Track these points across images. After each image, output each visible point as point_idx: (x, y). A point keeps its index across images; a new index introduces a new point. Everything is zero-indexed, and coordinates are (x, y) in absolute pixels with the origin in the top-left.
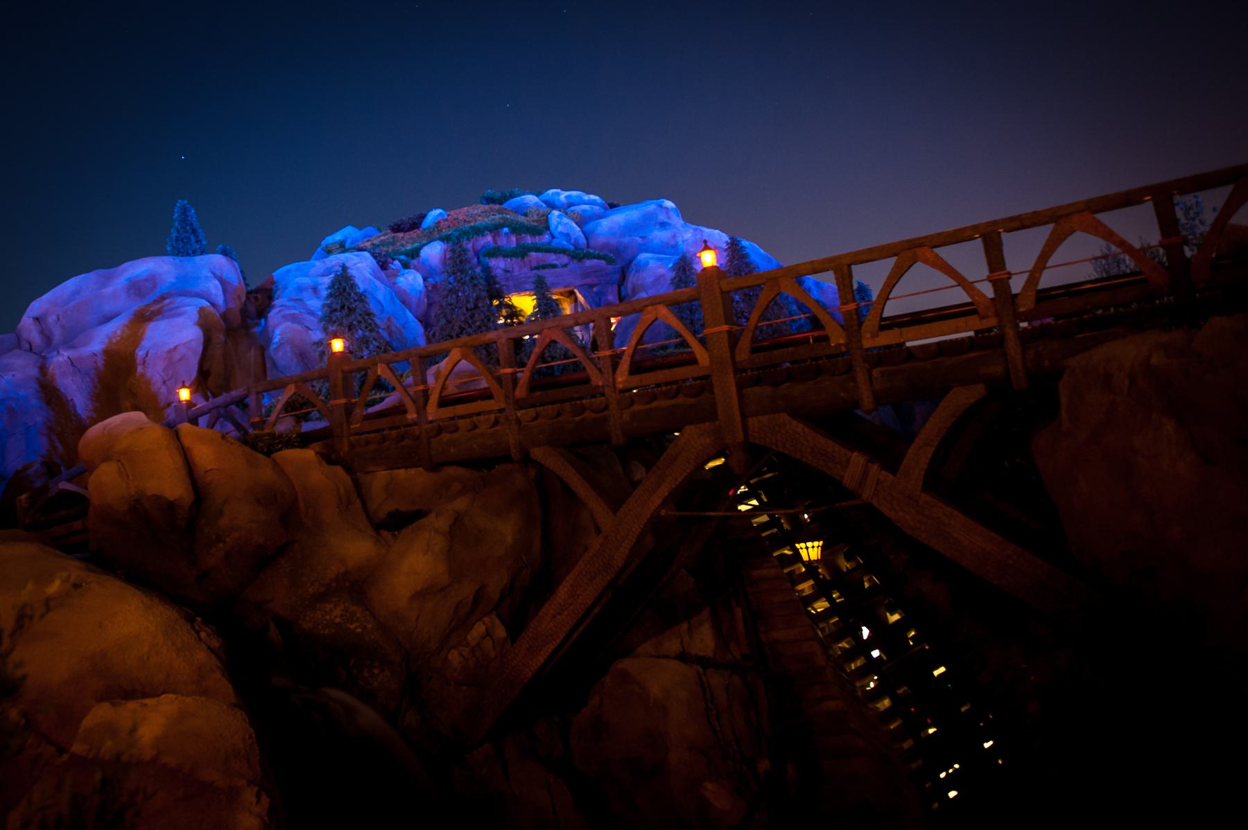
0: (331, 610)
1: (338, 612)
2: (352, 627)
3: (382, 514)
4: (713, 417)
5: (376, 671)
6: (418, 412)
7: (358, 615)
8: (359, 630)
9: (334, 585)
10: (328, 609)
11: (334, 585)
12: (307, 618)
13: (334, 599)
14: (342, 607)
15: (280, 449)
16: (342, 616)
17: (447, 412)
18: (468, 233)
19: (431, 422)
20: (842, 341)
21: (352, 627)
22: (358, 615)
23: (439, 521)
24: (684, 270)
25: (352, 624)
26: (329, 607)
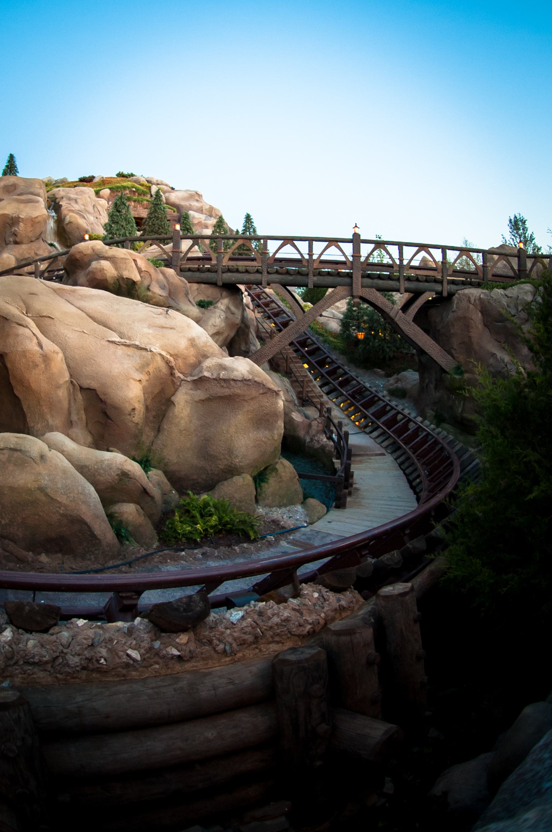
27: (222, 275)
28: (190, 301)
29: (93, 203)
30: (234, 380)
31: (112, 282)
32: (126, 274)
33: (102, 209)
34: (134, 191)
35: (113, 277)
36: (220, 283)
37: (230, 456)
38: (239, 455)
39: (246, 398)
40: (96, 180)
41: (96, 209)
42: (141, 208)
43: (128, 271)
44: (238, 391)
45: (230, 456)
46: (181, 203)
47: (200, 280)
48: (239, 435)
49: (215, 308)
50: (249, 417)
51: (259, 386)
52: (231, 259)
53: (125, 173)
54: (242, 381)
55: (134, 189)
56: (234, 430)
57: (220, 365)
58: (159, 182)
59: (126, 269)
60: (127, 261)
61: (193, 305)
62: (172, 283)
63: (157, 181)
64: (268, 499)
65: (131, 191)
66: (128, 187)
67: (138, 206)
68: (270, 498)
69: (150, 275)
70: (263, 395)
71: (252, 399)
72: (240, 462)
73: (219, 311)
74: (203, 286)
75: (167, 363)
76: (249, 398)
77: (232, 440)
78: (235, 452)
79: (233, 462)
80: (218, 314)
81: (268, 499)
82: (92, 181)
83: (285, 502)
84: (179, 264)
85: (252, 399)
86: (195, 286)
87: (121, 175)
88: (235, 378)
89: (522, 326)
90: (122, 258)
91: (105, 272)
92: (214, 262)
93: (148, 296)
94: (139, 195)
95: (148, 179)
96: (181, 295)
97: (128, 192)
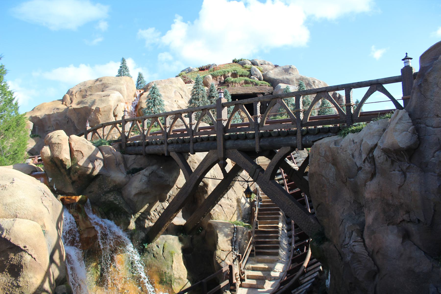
0: (110, 196)
1: (113, 197)
2: (116, 202)
3: (131, 168)
7: (118, 199)
8: (118, 203)
9: (112, 189)
10: (110, 196)
11: (112, 189)
12: (103, 198)
13: (112, 193)
14: (114, 196)
16: (113, 198)
21: (116, 202)
22: (118, 199)
25: (116, 201)
26: (110, 195)
28: (120, 170)
35: (48, 157)
49: (139, 174)
53: (237, 59)
74: (139, 156)
86: (133, 157)
89: (409, 165)
95: (253, 62)
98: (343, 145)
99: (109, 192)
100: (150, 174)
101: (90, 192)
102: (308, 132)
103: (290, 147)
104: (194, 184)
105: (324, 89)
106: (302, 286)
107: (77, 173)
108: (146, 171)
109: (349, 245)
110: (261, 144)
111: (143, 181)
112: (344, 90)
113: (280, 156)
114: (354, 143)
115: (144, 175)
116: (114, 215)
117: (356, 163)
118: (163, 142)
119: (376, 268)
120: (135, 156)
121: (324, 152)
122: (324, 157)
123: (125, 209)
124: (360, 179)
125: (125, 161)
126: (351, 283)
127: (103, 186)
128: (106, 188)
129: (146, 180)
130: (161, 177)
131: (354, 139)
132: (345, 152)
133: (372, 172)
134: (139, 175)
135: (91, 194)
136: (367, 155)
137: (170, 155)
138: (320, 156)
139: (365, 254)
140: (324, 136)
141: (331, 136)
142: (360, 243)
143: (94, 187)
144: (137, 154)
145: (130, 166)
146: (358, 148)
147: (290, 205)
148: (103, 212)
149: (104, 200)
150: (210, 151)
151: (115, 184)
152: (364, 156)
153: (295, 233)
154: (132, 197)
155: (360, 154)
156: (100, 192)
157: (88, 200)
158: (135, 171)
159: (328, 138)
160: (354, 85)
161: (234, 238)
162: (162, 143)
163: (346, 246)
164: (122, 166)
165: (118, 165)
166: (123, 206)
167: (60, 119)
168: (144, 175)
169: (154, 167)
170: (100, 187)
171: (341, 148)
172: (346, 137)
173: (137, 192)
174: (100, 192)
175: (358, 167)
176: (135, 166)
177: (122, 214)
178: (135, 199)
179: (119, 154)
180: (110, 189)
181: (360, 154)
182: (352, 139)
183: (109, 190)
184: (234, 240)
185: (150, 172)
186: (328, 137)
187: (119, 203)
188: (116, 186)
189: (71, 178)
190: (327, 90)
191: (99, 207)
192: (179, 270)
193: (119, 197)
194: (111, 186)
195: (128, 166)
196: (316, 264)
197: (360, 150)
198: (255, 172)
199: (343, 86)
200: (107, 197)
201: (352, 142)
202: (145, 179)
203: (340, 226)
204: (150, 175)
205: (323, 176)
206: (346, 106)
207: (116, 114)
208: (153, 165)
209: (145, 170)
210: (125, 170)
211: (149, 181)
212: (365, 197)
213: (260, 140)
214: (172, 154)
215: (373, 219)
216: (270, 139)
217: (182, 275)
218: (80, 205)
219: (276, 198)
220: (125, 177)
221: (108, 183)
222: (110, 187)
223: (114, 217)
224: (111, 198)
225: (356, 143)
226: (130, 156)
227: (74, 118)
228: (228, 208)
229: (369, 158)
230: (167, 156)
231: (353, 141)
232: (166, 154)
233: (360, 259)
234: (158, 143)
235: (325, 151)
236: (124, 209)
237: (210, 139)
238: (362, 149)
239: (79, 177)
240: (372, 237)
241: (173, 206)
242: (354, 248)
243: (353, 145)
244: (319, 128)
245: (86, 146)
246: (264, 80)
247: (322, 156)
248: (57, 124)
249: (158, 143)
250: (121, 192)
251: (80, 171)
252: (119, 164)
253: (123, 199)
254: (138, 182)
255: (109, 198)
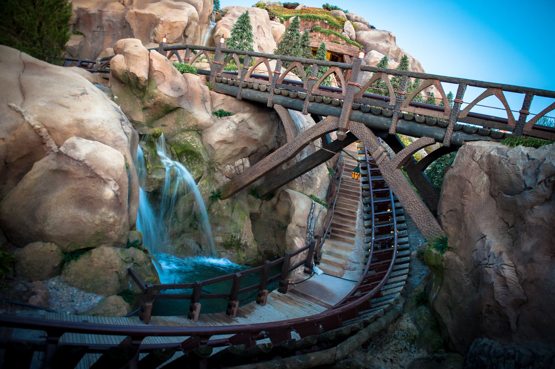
2: (193, 145)
3: (217, 109)
4: (339, 116)
5: (197, 162)
6: (241, 76)
8: (195, 147)
9: (191, 128)
11: (191, 128)
15: (188, 72)
17: (252, 80)
18: (311, 17)
19: (245, 82)
20: (393, 104)
23: (235, 118)
24: (384, 62)
27: (241, 90)
29: (258, 24)
30: (72, 158)
31: (121, 74)
32: (133, 69)
33: (268, 31)
34: (326, 23)
36: (239, 97)
37: (43, 222)
38: (50, 224)
39: (75, 177)
40: (299, 8)
41: (260, 30)
42: (327, 40)
43: (136, 67)
44: (71, 169)
45: (43, 222)
46: (369, 42)
47: (226, 92)
48: (58, 207)
49: (228, 118)
50: (73, 194)
51: (88, 169)
52: (320, 88)
54: (77, 161)
55: (326, 22)
56: (55, 201)
57: (74, 144)
58: (358, 19)
59: (134, 65)
60: (138, 58)
61: (207, 112)
62: (192, 89)
63: (357, 17)
64: (70, 276)
65: (323, 23)
66: (319, 18)
67: (324, 37)
68: (73, 277)
69: (164, 76)
70: (90, 179)
71: (80, 179)
72: (50, 230)
73: (230, 122)
74: (230, 98)
75: (36, 132)
76: (77, 177)
77: (50, 209)
78: (48, 221)
79: (44, 229)
80: (227, 124)
81: (70, 276)
82: (294, 9)
83: (88, 287)
84: (215, 75)
85: (80, 179)
86: (222, 96)
87: (327, 8)
88: (74, 157)
90: (134, 55)
91: (115, 64)
92: (239, 77)
93: (154, 93)
94: (331, 28)
96: (198, 101)
97: (319, 23)
98: (510, 156)
99: (188, 130)
100: (240, 122)
101: (164, 126)
102: (462, 129)
103: (433, 139)
104: (297, 148)
105: (499, 86)
106: (390, 286)
107: (154, 99)
108: (236, 117)
109: (494, 265)
110: (398, 125)
111: (231, 128)
112: (524, 95)
113: (418, 146)
114: (529, 159)
115: (234, 122)
116: (187, 159)
117: (524, 181)
118: (268, 90)
119: (525, 298)
120: (224, 95)
121: (479, 157)
122: (478, 162)
123: (202, 155)
124: (525, 200)
125: (212, 100)
126: (489, 306)
127: (181, 122)
128: (184, 125)
129: (234, 128)
130: (250, 128)
131: (529, 154)
132: (511, 165)
133: (547, 197)
134: (227, 120)
135: (164, 127)
136: (547, 178)
137: (274, 107)
138: (474, 160)
139: (515, 281)
140: (482, 138)
141: (489, 141)
142: (511, 268)
143: (170, 121)
144: (227, 95)
145: (217, 106)
146: (535, 167)
147: (414, 202)
148: (175, 153)
149: (179, 139)
150: (329, 117)
151: (196, 124)
152: (541, 177)
153: (375, 225)
154: (213, 143)
155: (536, 174)
156: (176, 128)
157: (162, 136)
158: (221, 114)
159: (486, 142)
160: (539, 91)
161: (311, 214)
162: (266, 91)
163: (491, 266)
164: (208, 104)
165: (204, 101)
166: (201, 151)
167: (115, 20)
168: (234, 122)
169: (246, 116)
170: (177, 123)
171: (506, 159)
172: (515, 148)
173: (221, 140)
174: (176, 128)
175: (526, 185)
176: (226, 110)
177: (198, 160)
178: (217, 147)
179: (207, 88)
180: (189, 128)
181: (536, 174)
182: (525, 153)
183: (187, 128)
184: (311, 217)
185: (241, 120)
186: (485, 140)
187: (197, 146)
188: (196, 126)
189: (143, 103)
190: (503, 88)
191: (171, 146)
192: (246, 236)
193: (197, 140)
194: (191, 124)
195: (215, 106)
196: (402, 265)
197: (538, 169)
198: (381, 155)
199: (525, 89)
200: (183, 136)
201: (526, 158)
202: (233, 127)
203: (478, 241)
204: (240, 124)
205: (470, 182)
206: (520, 113)
207: (186, 34)
208: (244, 112)
209: (235, 116)
210: (211, 110)
211: (237, 130)
212: (526, 220)
213: (397, 121)
214: (276, 107)
215: (533, 247)
216: (412, 123)
217: (248, 242)
218: (153, 139)
219: (398, 189)
220: (210, 119)
221: (188, 120)
222: (189, 126)
223: (186, 161)
224: (188, 138)
225: (533, 159)
226: (217, 94)
227: (134, 24)
228: (307, 180)
229: (549, 180)
230: (269, 108)
231: (528, 156)
232: (269, 105)
233: (508, 284)
234: (261, 89)
235: (482, 156)
236: (201, 155)
237: (332, 103)
238: (541, 168)
239: (155, 104)
240: (529, 265)
241: (262, 166)
242: (503, 272)
243: (527, 161)
244: (404, 114)
245: (170, 69)
246: (356, 40)
247: (476, 161)
248: (109, 25)
249: (262, 90)
250: (200, 135)
251: (159, 98)
252: (205, 101)
253: (202, 143)
254: (225, 128)
255: (185, 138)
